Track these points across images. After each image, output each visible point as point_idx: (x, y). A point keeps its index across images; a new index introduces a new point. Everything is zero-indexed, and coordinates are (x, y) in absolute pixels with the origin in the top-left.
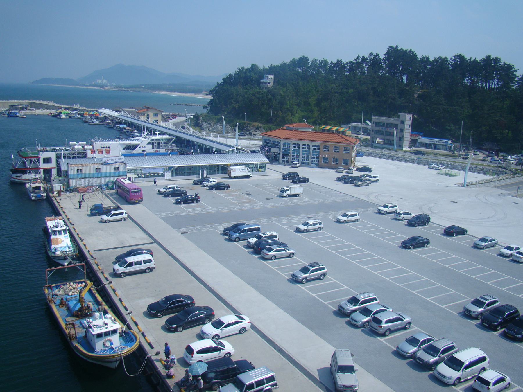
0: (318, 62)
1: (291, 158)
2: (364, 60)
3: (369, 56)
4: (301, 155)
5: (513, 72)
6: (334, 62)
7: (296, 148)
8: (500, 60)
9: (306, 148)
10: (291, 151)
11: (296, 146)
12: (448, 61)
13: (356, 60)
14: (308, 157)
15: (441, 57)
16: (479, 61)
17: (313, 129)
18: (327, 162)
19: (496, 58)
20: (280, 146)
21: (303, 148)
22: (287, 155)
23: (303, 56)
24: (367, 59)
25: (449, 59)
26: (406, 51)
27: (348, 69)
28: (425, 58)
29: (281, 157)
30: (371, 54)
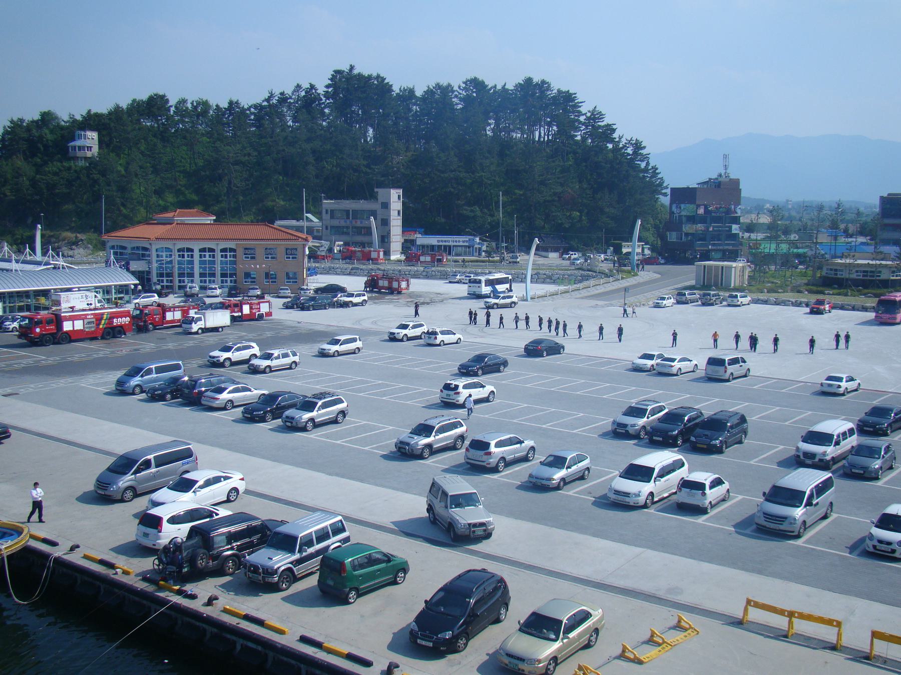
0: (189, 106)
2: (283, 99)
3: (294, 91)
5: (576, 106)
6: (221, 106)
7: (186, 258)
8: (549, 86)
9: (207, 256)
11: (186, 254)
12: (454, 91)
13: (268, 100)
14: (213, 275)
15: (441, 84)
16: (513, 88)
18: (254, 282)
19: (543, 82)
20: (149, 256)
22: (169, 275)
23: (155, 92)
24: (291, 98)
25: (456, 88)
26: (370, 77)
27: (253, 120)
28: (406, 90)
30: (298, 87)
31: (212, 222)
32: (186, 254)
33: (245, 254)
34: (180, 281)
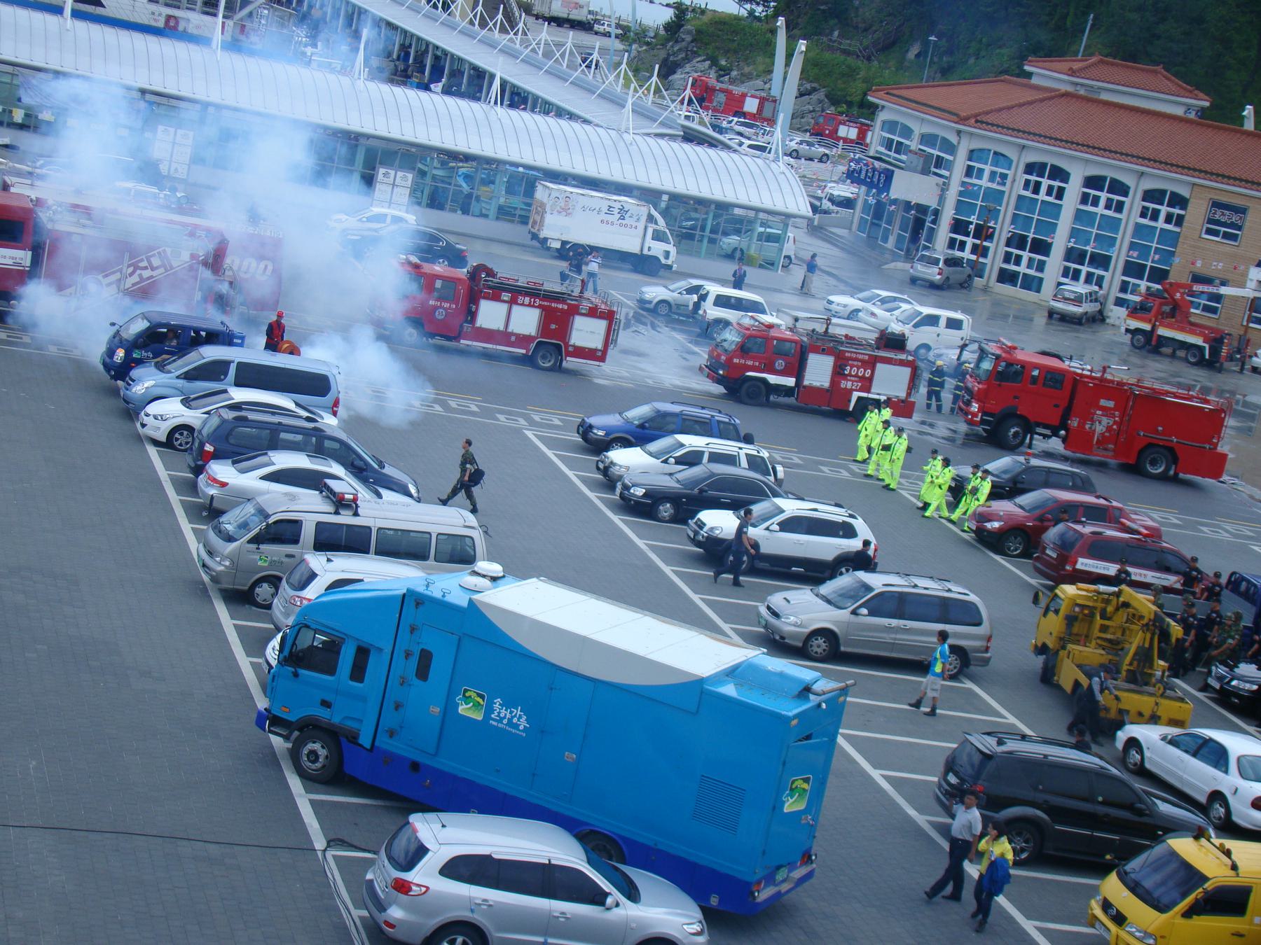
1: (1003, 248)
4: (1060, 241)
7: (1042, 196)
9: (1102, 203)
10: (1007, 210)
11: (1045, 183)
14: (1102, 261)
17: (1202, 113)
20: (949, 166)
21: (1085, 199)
29: (943, 232)
31: (1192, 116)
32: (1045, 183)
33: (1210, 221)
34: (1007, 258)
